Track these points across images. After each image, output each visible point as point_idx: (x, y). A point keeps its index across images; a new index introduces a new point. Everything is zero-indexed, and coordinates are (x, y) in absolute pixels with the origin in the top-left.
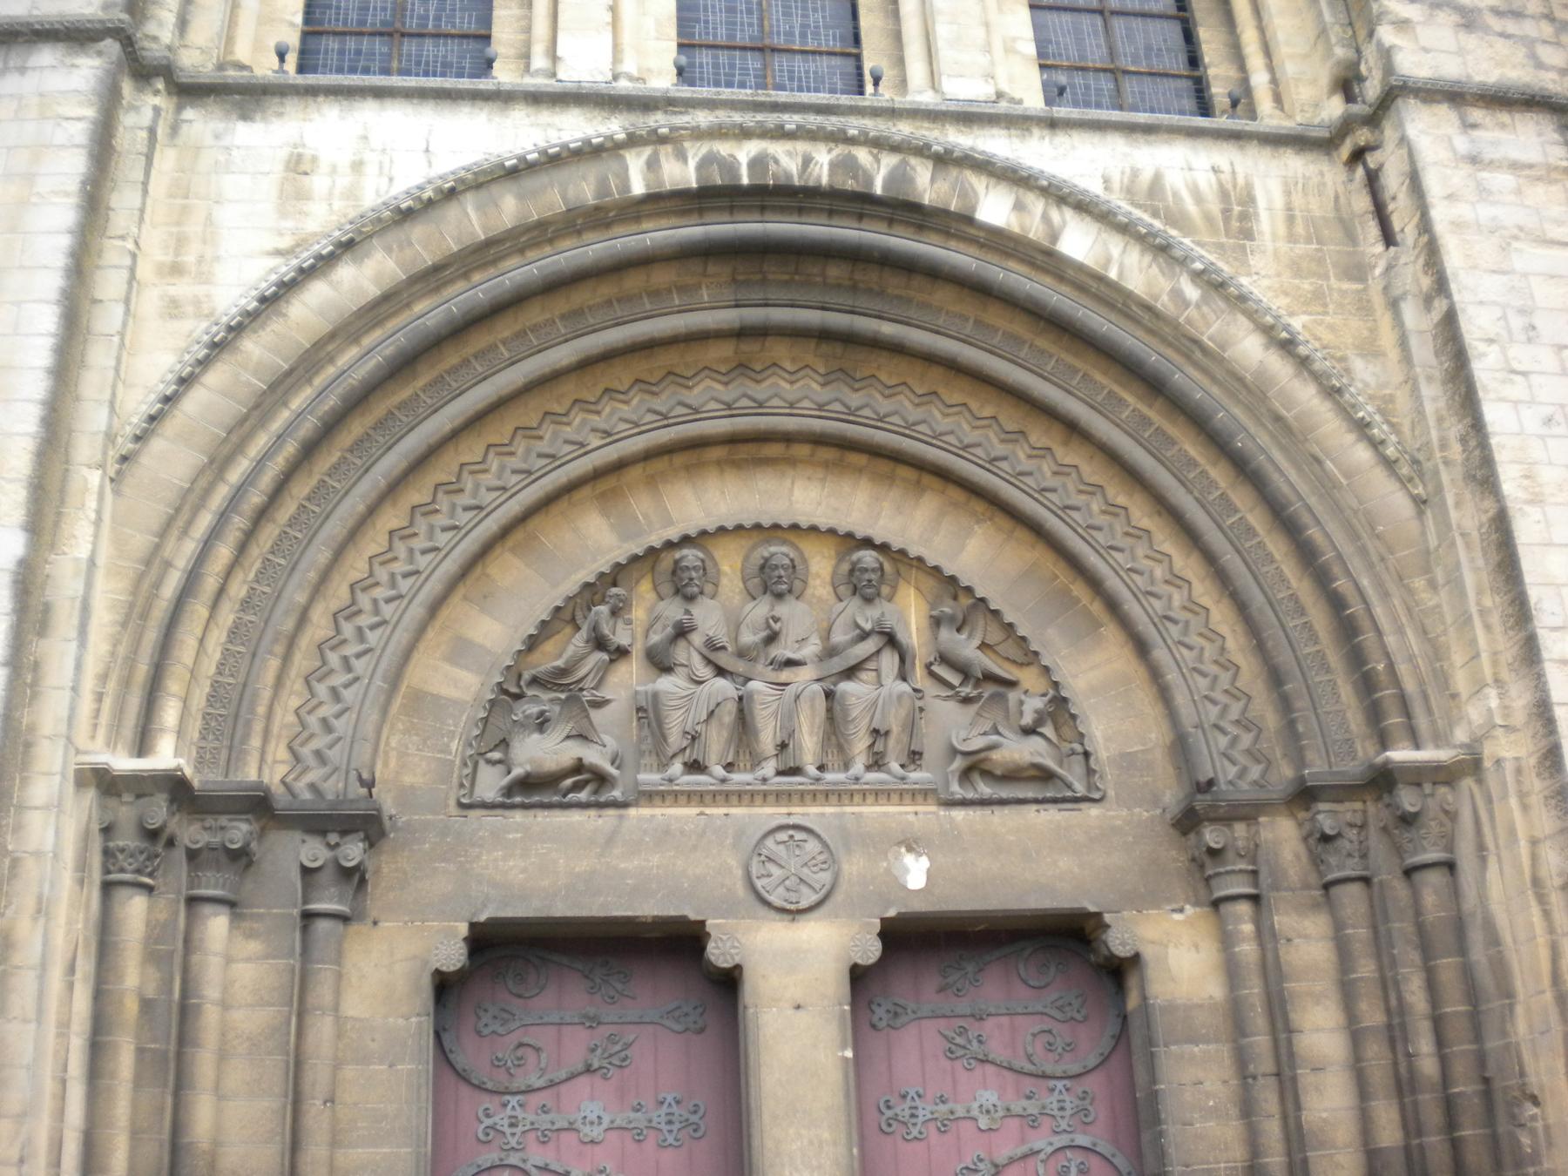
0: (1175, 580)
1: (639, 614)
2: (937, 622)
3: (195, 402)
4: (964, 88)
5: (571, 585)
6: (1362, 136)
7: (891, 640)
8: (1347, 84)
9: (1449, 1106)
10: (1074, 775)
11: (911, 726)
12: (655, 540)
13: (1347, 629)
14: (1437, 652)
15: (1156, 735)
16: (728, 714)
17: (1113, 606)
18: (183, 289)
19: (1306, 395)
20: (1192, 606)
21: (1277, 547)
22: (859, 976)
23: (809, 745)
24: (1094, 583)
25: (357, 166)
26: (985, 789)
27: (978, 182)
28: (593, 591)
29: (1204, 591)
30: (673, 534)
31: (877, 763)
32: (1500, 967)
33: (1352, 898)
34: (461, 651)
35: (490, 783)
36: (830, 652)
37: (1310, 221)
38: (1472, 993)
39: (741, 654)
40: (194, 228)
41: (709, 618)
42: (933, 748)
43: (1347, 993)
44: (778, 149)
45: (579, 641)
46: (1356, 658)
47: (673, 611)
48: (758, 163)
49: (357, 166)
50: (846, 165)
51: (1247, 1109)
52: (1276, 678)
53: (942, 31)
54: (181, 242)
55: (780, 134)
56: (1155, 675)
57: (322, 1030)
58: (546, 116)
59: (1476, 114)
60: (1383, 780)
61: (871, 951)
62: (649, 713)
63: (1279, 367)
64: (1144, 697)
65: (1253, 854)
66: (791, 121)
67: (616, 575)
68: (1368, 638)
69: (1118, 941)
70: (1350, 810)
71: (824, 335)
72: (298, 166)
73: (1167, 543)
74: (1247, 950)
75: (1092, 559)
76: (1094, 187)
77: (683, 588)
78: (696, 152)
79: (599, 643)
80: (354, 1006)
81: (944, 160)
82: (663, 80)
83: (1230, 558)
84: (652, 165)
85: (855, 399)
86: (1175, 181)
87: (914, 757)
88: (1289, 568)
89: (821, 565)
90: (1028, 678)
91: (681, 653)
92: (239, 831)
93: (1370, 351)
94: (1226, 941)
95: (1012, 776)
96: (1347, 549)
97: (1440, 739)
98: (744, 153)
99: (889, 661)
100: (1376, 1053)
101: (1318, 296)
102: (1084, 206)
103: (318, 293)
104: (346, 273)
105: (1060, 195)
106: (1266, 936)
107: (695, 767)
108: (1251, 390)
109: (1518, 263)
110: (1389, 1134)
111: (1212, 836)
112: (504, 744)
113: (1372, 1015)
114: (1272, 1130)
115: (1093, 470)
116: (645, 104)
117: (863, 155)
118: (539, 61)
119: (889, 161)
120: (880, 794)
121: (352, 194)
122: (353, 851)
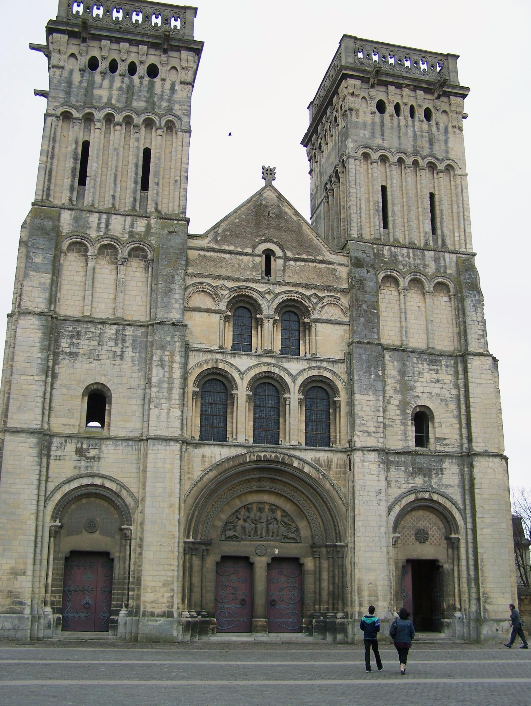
0: (315, 514)
1: (242, 513)
2: (282, 516)
3: (193, 492)
4: (294, 443)
5: (234, 510)
6: (349, 453)
7: (276, 519)
8: (350, 442)
9: (338, 586)
10: (298, 539)
11: (278, 532)
12: (245, 504)
13: (335, 526)
14: (345, 530)
15: (310, 534)
16: (254, 529)
17: (306, 517)
18: (190, 476)
19: (334, 493)
20: (316, 518)
21: (327, 512)
22: (269, 565)
23: (264, 533)
24: (304, 514)
25: (211, 457)
26: (287, 540)
27: (294, 459)
28: (237, 511)
29: (318, 517)
30: (248, 503)
31: (273, 536)
32: (346, 571)
33: (331, 559)
34: (220, 519)
35: (223, 537)
36: (268, 520)
37: (340, 465)
38: (343, 574)
39: (256, 520)
40: (190, 466)
41: (252, 516)
42: (280, 534)
43: (329, 572)
44: (267, 454)
45: (235, 517)
46: (335, 530)
47: (247, 514)
48: (264, 456)
49: (211, 457)
50: (276, 457)
51: (315, 584)
52: (325, 530)
53: (292, 432)
54: (189, 468)
55: (267, 452)
56: (310, 527)
57: (204, 570)
58: (237, 449)
59: (366, 452)
60: (336, 546)
61: (270, 561)
62: (244, 528)
63: (331, 488)
64: (309, 530)
65: (320, 552)
66: (269, 450)
67: (240, 509)
68: (337, 528)
69: (301, 561)
70: (332, 549)
71: (271, 478)
72: (203, 456)
73: (314, 509)
74: (317, 564)
75: (304, 511)
76: (309, 460)
77: (249, 510)
78: (256, 454)
79: (237, 518)
80: (208, 566)
81: (290, 456)
82: (251, 440)
83: (322, 514)
84: (250, 456)
85: (274, 485)
86: (321, 459)
87: (277, 536)
88: (329, 515)
89: (267, 507)
90: (294, 525)
91: (248, 520)
92: (197, 546)
93: (344, 486)
94: (315, 563)
95: (290, 538)
96: (336, 515)
97: (344, 542)
98: (262, 454)
99: (275, 522)
100: (331, 579)
101: (339, 477)
102: (308, 464)
103: (207, 476)
104: (210, 473)
105: (305, 462)
106: (320, 562)
107: (250, 536)
108: (328, 492)
109: (365, 478)
110: (331, 589)
111: (315, 550)
112: (225, 532)
113: (331, 575)
114: (318, 587)
115: (305, 498)
116: (249, 447)
117: (278, 455)
118: (234, 437)
119: (282, 456)
120: (273, 541)
121: (211, 461)
122: (209, 548)
